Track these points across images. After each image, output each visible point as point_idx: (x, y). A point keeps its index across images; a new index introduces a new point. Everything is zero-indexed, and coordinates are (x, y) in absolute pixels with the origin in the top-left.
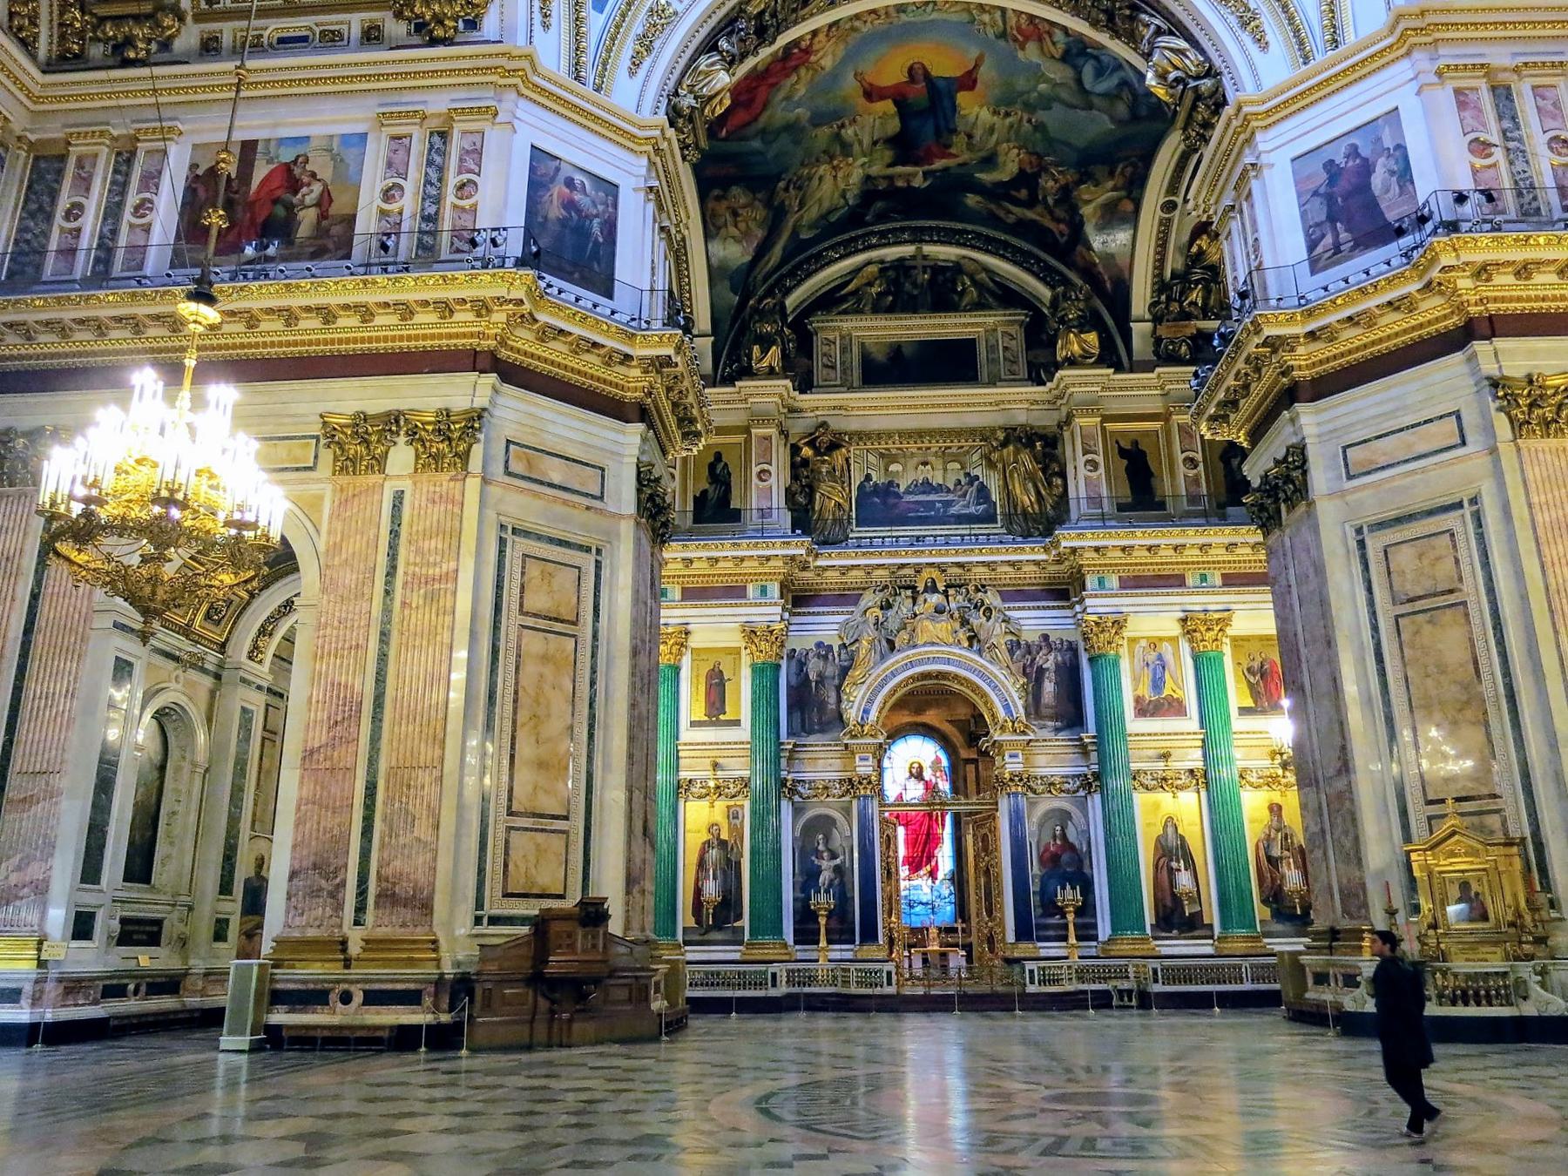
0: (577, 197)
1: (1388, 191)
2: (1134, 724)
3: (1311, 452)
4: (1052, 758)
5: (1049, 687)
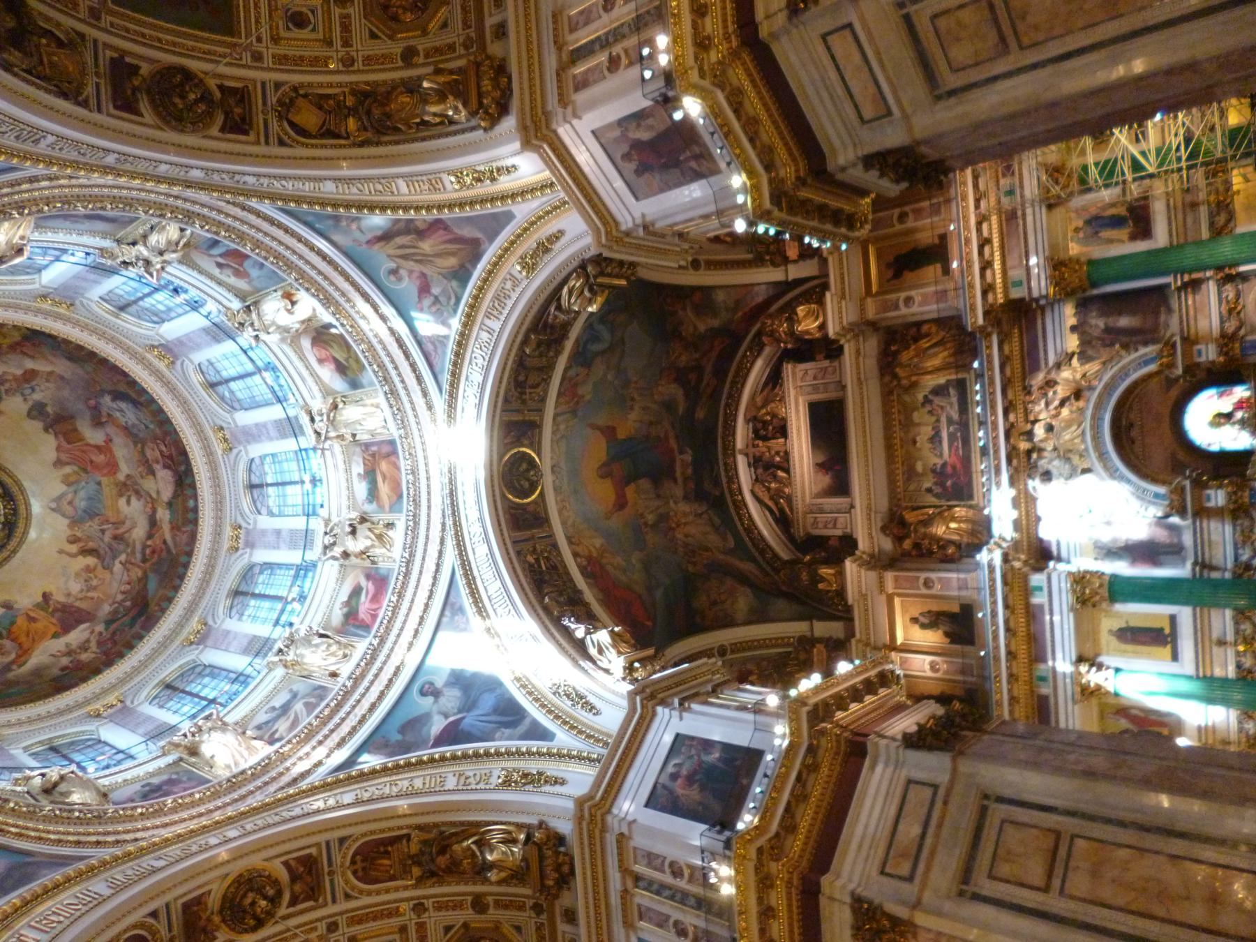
0: (684, 772)
1: (651, 127)
5: (1124, 322)
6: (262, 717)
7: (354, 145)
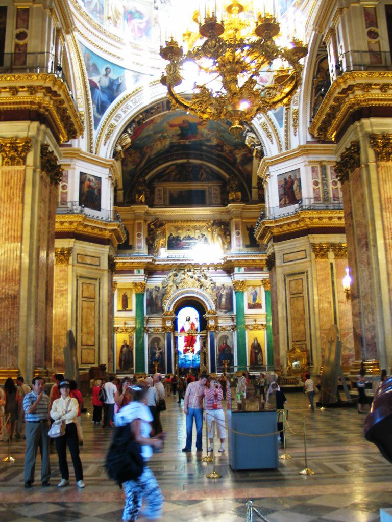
0: (91, 184)
2: (247, 311)
3: (276, 255)
4: (225, 322)
5: (224, 300)
7: (314, 78)
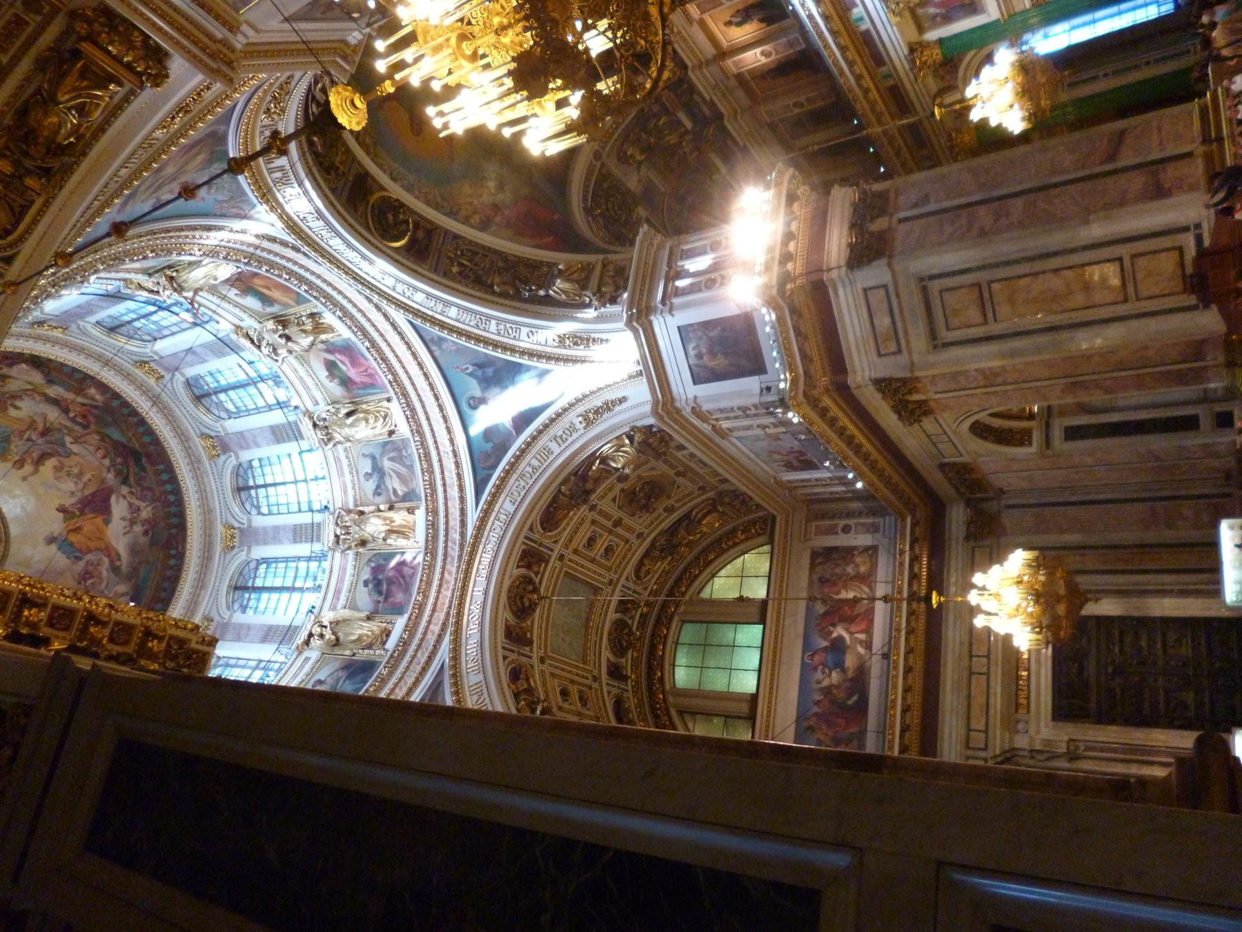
0: (704, 350)
6: (370, 485)
